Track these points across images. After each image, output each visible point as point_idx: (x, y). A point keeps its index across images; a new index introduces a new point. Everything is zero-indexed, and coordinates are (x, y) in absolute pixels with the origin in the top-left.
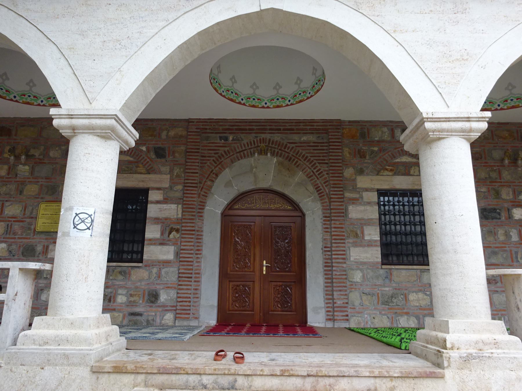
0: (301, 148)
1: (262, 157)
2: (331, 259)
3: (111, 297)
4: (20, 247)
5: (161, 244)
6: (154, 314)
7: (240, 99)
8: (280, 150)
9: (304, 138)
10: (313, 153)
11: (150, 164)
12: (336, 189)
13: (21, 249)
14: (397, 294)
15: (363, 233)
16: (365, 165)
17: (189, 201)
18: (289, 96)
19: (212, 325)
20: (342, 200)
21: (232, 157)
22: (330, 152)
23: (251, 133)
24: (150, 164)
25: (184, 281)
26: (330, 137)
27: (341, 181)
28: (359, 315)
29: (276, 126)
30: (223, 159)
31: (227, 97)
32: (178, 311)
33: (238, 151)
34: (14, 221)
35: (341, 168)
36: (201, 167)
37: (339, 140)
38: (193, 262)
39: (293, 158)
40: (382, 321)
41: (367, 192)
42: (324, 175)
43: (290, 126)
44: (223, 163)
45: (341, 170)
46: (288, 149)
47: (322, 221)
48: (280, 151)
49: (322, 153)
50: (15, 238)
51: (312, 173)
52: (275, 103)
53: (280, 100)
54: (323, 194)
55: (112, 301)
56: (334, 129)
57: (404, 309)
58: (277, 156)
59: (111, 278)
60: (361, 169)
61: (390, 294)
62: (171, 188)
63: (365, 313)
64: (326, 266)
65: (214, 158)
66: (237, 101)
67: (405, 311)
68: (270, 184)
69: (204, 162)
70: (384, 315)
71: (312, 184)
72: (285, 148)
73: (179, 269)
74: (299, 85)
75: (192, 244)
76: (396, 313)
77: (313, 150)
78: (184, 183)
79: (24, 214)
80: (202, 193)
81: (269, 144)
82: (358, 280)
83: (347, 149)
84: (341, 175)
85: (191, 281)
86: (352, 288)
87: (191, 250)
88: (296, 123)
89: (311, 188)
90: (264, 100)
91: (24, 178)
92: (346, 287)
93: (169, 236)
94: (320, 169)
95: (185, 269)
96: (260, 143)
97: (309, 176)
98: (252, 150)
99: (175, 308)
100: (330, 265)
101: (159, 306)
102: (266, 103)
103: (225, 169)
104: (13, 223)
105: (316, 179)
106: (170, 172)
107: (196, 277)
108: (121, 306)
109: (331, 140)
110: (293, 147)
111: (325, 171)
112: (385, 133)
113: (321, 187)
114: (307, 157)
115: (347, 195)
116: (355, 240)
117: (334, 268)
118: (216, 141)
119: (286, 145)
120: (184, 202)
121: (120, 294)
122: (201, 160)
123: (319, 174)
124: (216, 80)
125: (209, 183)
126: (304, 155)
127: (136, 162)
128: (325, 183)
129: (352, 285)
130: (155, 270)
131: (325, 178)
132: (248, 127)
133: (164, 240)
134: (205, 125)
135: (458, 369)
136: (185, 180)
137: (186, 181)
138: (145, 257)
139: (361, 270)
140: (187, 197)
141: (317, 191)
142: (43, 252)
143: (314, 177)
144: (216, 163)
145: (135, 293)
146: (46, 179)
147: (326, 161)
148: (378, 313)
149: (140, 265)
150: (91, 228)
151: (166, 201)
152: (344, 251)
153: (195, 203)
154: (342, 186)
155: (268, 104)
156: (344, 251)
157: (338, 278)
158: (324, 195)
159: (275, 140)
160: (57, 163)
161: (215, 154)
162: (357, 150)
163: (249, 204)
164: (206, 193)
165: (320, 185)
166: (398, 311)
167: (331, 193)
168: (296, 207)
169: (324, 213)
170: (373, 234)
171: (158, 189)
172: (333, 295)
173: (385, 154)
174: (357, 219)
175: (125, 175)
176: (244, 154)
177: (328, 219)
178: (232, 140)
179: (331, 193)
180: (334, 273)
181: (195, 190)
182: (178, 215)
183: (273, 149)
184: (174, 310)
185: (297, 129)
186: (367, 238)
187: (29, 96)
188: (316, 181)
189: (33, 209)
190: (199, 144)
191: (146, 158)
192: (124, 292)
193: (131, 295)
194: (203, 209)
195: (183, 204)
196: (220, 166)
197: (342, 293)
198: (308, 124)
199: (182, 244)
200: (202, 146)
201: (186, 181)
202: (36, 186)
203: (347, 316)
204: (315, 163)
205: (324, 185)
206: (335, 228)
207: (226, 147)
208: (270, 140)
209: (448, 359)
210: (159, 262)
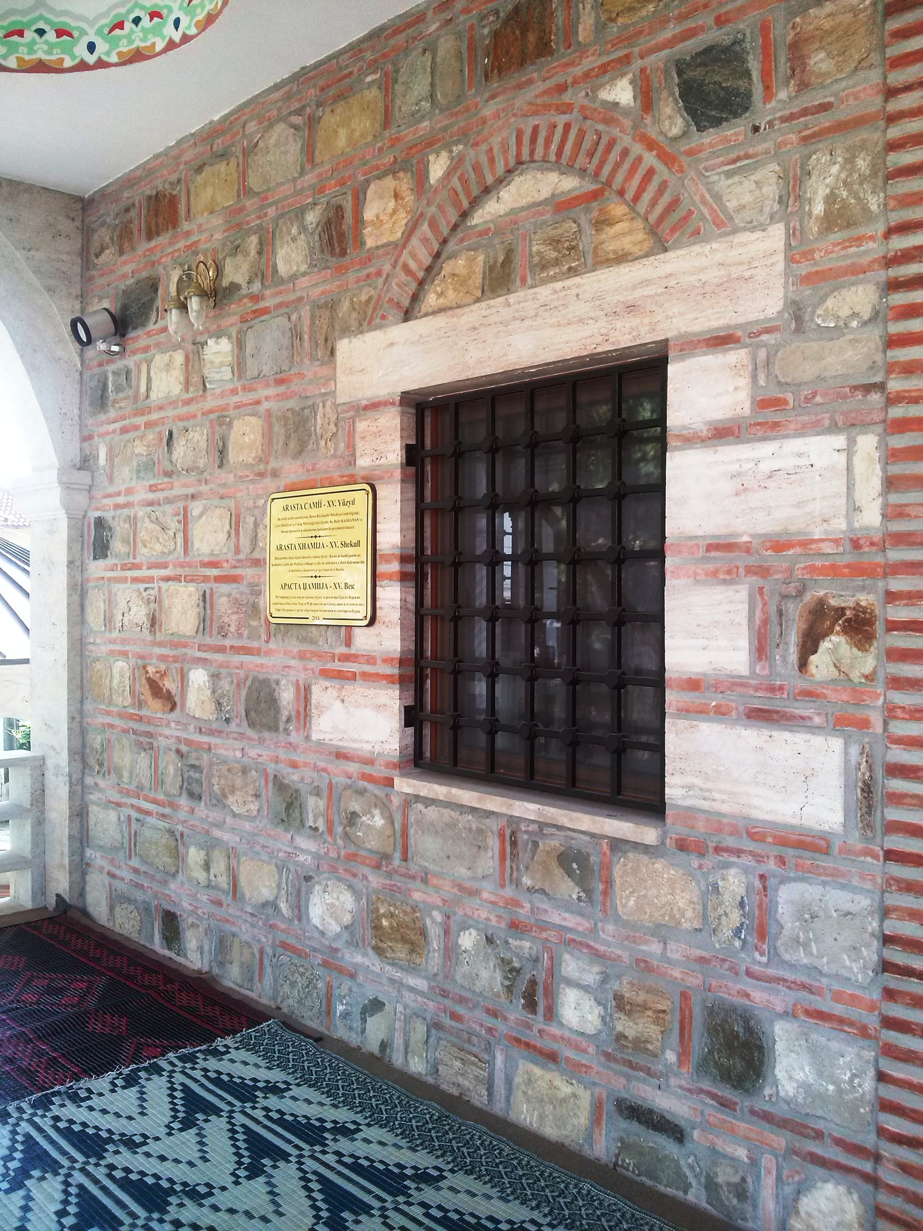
3: (533, 983)
4: (238, 686)
5: (761, 716)
6: (741, 1153)
11: (663, 186)
13: (244, 693)
24: (663, 186)
34: (218, 579)
50: (221, 649)
55: (541, 1009)
59: (527, 881)
62: (798, 318)
78: (891, 261)
79: (237, 551)
91: (222, 395)
93: (803, 664)
99: (867, 1166)
101: (766, 1117)
104: (215, 585)
108: (577, 1048)
120: (897, 412)
121: (571, 983)
127: (595, 195)
133: (772, 689)
142: (298, 712)
145: (641, 997)
146: (280, 382)
149: (648, 834)
151: (770, 415)
160: (300, 299)
171: (721, 341)
175: (544, 292)
182: (854, 508)
187: (137, 21)
189: (256, 525)
191: (637, 149)
192: (591, 977)
193: (621, 1004)
202: (253, 420)
210: (756, 832)
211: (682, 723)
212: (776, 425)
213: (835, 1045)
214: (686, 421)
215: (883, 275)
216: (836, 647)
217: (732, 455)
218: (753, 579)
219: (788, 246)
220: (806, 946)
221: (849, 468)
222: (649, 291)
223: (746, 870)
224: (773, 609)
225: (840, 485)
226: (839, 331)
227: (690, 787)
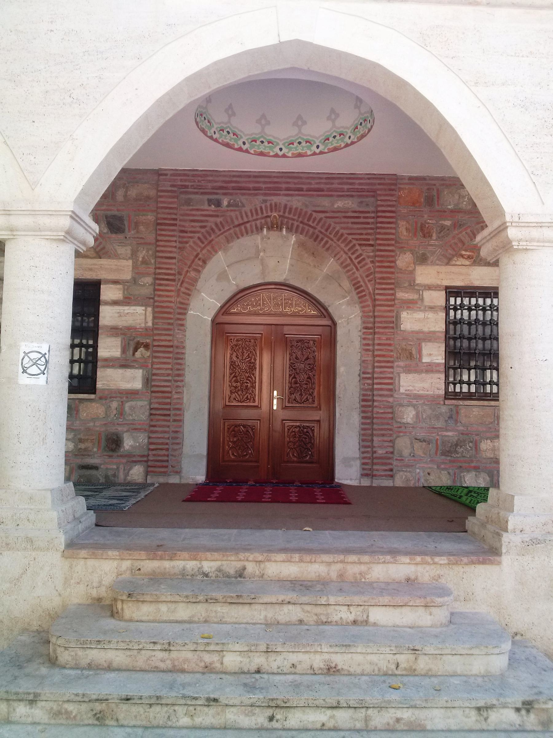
0: (333, 220)
1: (274, 234)
2: (372, 390)
7: (240, 143)
8: (301, 222)
9: (340, 204)
10: (351, 229)
12: (384, 286)
14: (464, 441)
15: (420, 352)
16: (430, 248)
17: (163, 302)
18: (317, 138)
19: (200, 482)
20: (393, 303)
21: (227, 233)
22: (378, 228)
23: (256, 195)
25: (158, 420)
26: (379, 203)
27: (393, 273)
28: (408, 470)
29: (295, 184)
30: (213, 236)
31: (220, 141)
32: (150, 463)
33: (236, 223)
35: (393, 254)
36: (180, 248)
37: (393, 209)
38: (171, 392)
39: (321, 236)
40: (439, 478)
41: (431, 292)
42: (366, 264)
43: (317, 183)
44: (213, 242)
45: (392, 256)
46: (313, 222)
47: (360, 334)
48: (301, 225)
49: (365, 229)
51: (349, 261)
52: (296, 148)
53: (304, 144)
54: (363, 294)
56: (385, 190)
57: (472, 461)
58: (296, 232)
60: (424, 255)
61: (454, 441)
63: (417, 467)
64: (364, 400)
65: (199, 235)
66: (236, 147)
67: (473, 464)
68: (284, 277)
69: (185, 240)
70: (443, 469)
71: (348, 277)
72: (309, 220)
73: (150, 404)
74: (333, 121)
75: (170, 366)
76: (461, 467)
77: (352, 223)
80: (183, 289)
81: (284, 212)
82: (409, 420)
83: (404, 223)
84: (392, 264)
85: (169, 421)
86: (400, 432)
87: (168, 375)
88: (326, 178)
89: (346, 284)
90: (278, 144)
92: (391, 430)
93: (134, 354)
94: (361, 255)
95: (160, 403)
96: (271, 211)
97: (344, 264)
98: (258, 222)
100: (370, 398)
102: (281, 149)
103: (216, 252)
105: (355, 270)
106: (132, 255)
107: (175, 415)
109: (380, 209)
110: (321, 219)
111: (369, 257)
113: (362, 283)
114: (342, 235)
115: (401, 295)
116: (408, 362)
117: (375, 404)
118: (202, 207)
119: (311, 215)
122: (180, 237)
123: (359, 263)
124: (204, 116)
125: (192, 274)
126: (337, 232)
128: (367, 276)
129: (400, 427)
130: (114, 405)
131: (369, 269)
132: (251, 185)
133: (126, 360)
134: (185, 180)
135: (518, 555)
136: (156, 268)
137: (158, 271)
138: (99, 385)
139: (414, 406)
140: (159, 296)
141: (356, 289)
143: (352, 266)
144: (203, 243)
147: (371, 242)
148: (436, 467)
149: (92, 396)
150: (45, 372)
151: (127, 301)
152: (391, 378)
153: (172, 305)
154: (393, 281)
155: (285, 150)
156: (391, 378)
157: (381, 418)
158: (365, 295)
159: (294, 207)
161: (202, 227)
162: (419, 225)
163: (253, 306)
164: (189, 289)
165: (360, 279)
166: (464, 465)
167: (377, 291)
168: (323, 311)
169: (364, 322)
170: (435, 353)
171: (115, 282)
172: (372, 441)
173: (461, 232)
176: (246, 228)
177: (371, 331)
178: (227, 206)
179: (377, 291)
180: (375, 410)
181: (172, 285)
183: (291, 222)
184: (145, 461)
185: (329, 190)
186: (425, 360)
188: (354, 273)
190: (175, 211)
194: (185, 314)
195: (154, 307)
196: (209, 248)
197: (385, 438)
198: (345, 180)
199: (155, 366)
200: (182, 215)
201: (158, 271)
203: (391, 470)
204: (354, 245)
205: (366, 280)
206: (379, 344)
207: (217, 216)
208: (286, 206)
209: (507, 544)
211: (102, 369)
212: (129, 303)
213: (138, 435)
214: (106, 299)
215: (154, 276)
216: (142, 350)
217: (117, 308)
218: (123, 336)
219: (133, 265)
220: (132, 415)
221: (145, 314)
222: (96, 267)
223: (118, 401)
224: (127, 343)
225: (143, 317)
226: (144, 285)
227: (103, 384)
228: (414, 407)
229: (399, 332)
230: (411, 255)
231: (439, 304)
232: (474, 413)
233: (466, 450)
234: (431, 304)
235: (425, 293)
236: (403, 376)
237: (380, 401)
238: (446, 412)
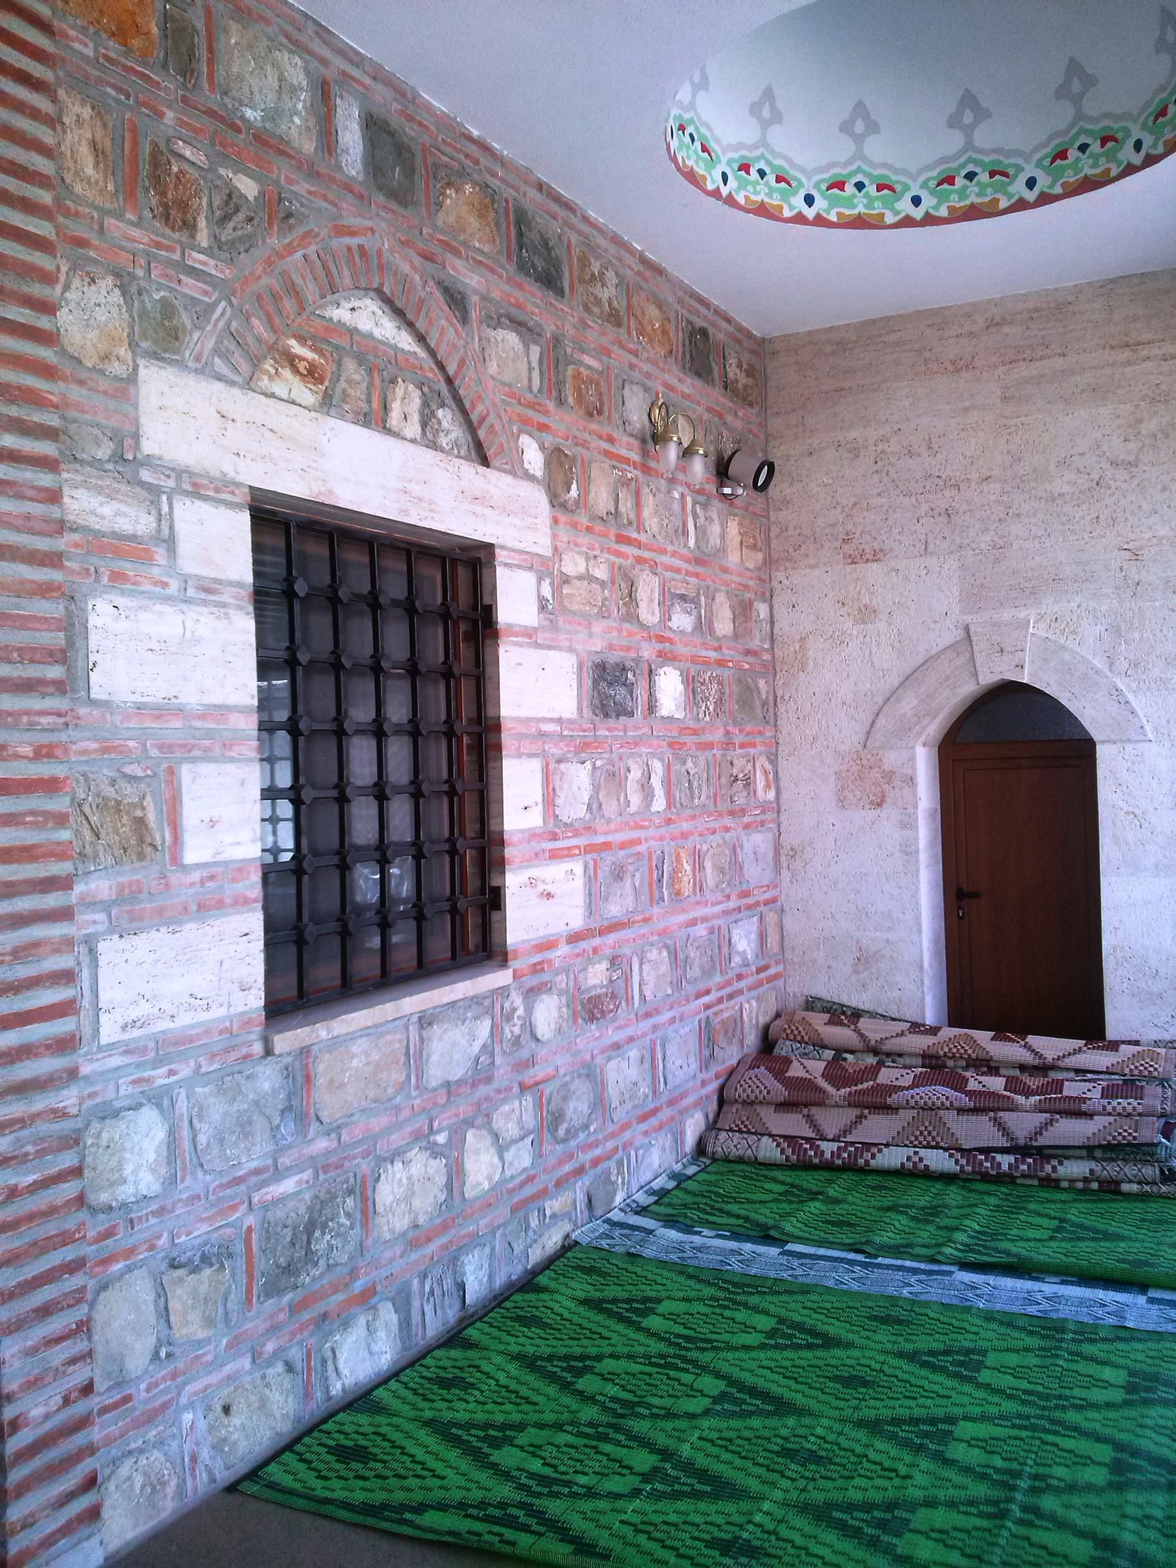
27: (47, 371)
60: (168, 310)
61: (302, 1210)
63: (183, 1400)
112: (294, 90)
129: (109, 1234)
139: (161, 1100)
154: (51, 419)
157: (30, 1217)
162: (146, 149)
173: (290, 249)
174: (140, 708)
228: (159, 1106)
229: (83, 711)
230: (116, 297)
231: (234, 576)
232: (355, 1063)
233: (338, 1235)
234: (204, 572)
235: (177, 505)
236: (108, 948)
237: (21, 1122)
238: (273, 1090)
